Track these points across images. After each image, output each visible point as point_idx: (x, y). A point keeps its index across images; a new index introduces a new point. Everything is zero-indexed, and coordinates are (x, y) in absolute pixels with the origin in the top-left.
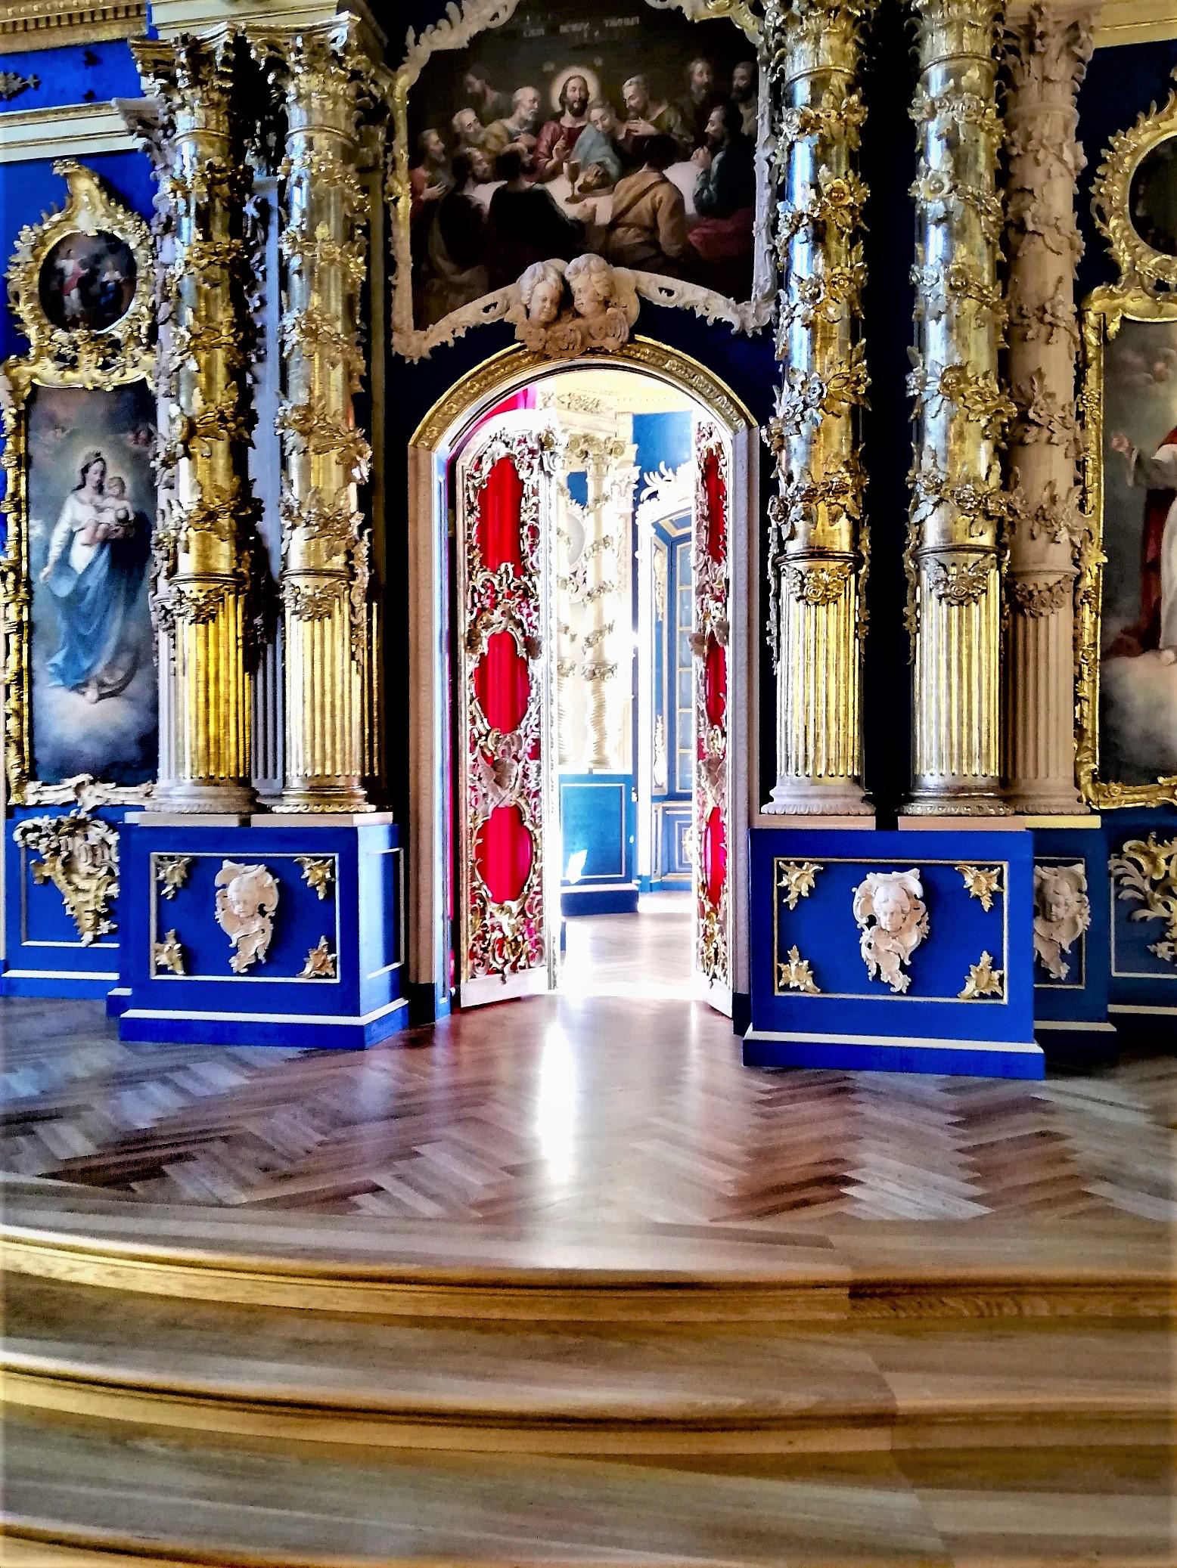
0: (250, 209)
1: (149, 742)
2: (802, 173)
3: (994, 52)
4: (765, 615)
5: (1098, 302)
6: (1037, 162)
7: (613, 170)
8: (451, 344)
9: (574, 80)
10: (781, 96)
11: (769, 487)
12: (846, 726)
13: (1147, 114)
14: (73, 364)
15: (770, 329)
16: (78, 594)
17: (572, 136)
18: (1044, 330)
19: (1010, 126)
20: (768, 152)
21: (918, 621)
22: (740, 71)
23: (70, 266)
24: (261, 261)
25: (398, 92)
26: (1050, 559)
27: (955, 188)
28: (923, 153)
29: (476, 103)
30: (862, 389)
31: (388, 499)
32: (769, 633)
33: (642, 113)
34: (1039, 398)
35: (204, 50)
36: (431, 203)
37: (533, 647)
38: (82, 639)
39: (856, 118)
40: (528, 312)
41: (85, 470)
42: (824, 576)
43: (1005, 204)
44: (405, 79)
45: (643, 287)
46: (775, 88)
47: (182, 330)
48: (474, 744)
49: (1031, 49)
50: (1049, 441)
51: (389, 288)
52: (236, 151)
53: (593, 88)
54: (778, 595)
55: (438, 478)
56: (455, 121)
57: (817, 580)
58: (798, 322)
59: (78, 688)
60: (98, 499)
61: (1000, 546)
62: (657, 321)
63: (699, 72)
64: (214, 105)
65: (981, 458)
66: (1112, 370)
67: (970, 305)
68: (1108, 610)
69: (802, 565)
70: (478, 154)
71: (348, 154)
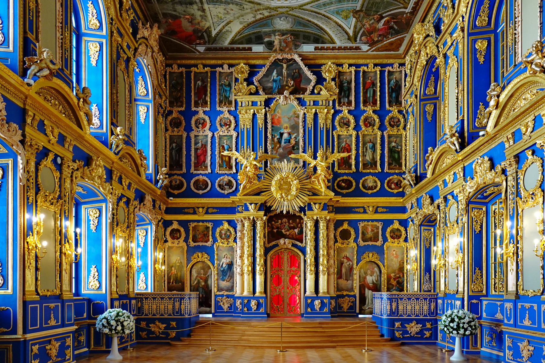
17: (285, 226)
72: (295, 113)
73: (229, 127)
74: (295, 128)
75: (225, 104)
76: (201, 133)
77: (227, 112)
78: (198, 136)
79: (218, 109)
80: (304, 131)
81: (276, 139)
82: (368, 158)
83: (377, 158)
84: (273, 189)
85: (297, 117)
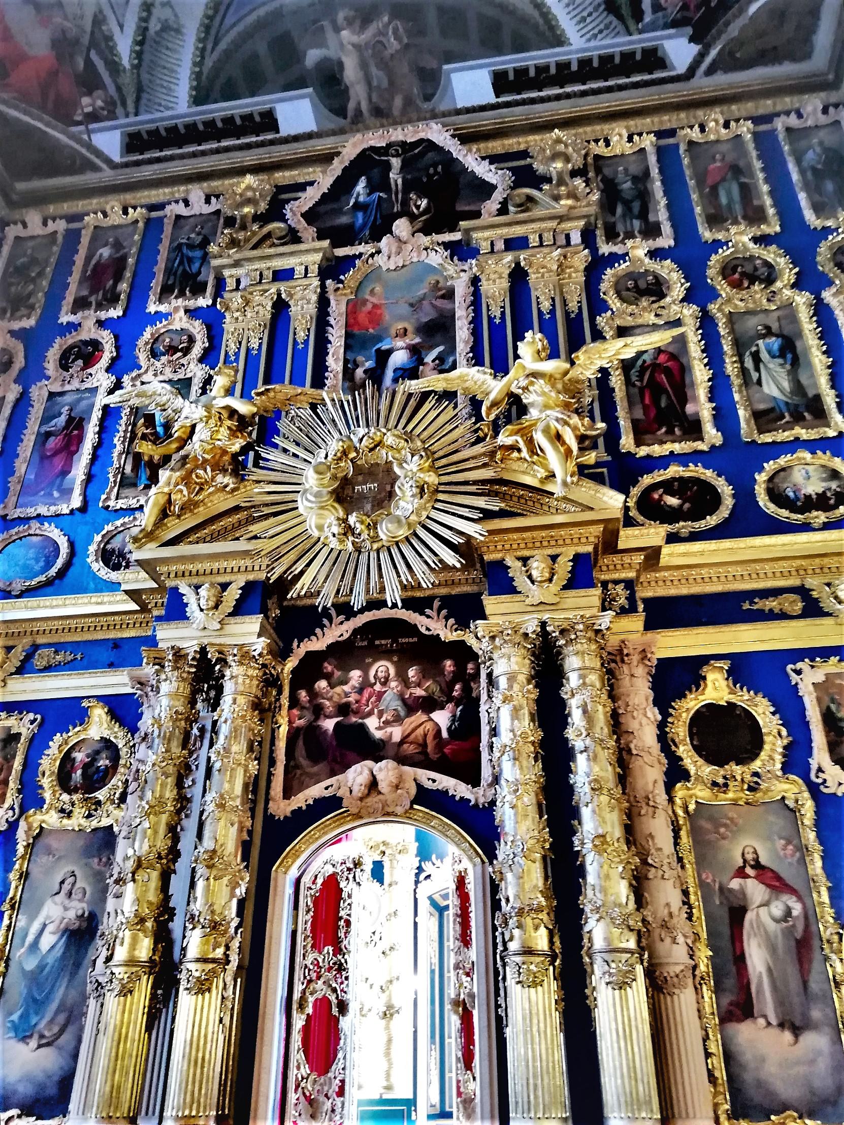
0: (195, 731)
1: (66, 1083)
2: (508, 721)
3: (602, 665)
4: (497, 994)
5: (680, 791)
6: (634, 718)
7: (402, 713)
8: (304, 808)
9: (382, 667)
10: (492, 681)
11: (496, 906)
12: (554, 1078)
13: (691, 691)
14: (69, 815)
15: (493, 803)
16: (41, 967)
17: (380, 695)
18: (651, 810)
19: (614, 701)
20: (487, 707)
21: (595, 999)
22: (470, 666)
23: (80, 756)
24: (196, 759)
25: (286, 671)
26: (675, 955)
27: (588, 735)
28: (569, 715)
29: (328, 677)
30: (547, 846)
31: (256, 908)
32: (500, 1006)
33: (419, 685)
34: (653, 851)
35: (183, 653)
36: (298, 729)
37: (343, 1007)
38: (35, 1001)
39: (533, 696)
40: (351, 791)
41: (62, 882)
42: (532, 967)
43: (618, 741)
44: (291, 664)
45: (418, 778)
46: (490, 675)
47: (144, 803)
48: (297, 1086)
49: (623, 661)
50: (663, 877)
51: (270, 775)
52: (192, 702)
53: (392, 671)
54: (504, 979)
55: (289, 890)
56: (316, 686)
57: (529, 970)
58: (507, 805)
59: (24, 1039)
60: (67, 902)
61: (641, 948)
62: (428, 798)
63: (448, 665)
64: (184, 680)
65: (622, 890)
66: (695, 832)
67: (604, 799)
68: (718, 990)
69: (518, 959)
70: (327, 703)
71: (256, 705)
72: (436, 286)
73: (185, 355)
74: (438, 329)
75: (182, 294)
76: (75, 384)
77: (182, 312)
78: (62, 394)
79: (152, 308)
80: (476, 333)
81: (359, 373)
82: (770, 389)
83: (816, 385)
84: (303, 505)
85: (443, 297)
